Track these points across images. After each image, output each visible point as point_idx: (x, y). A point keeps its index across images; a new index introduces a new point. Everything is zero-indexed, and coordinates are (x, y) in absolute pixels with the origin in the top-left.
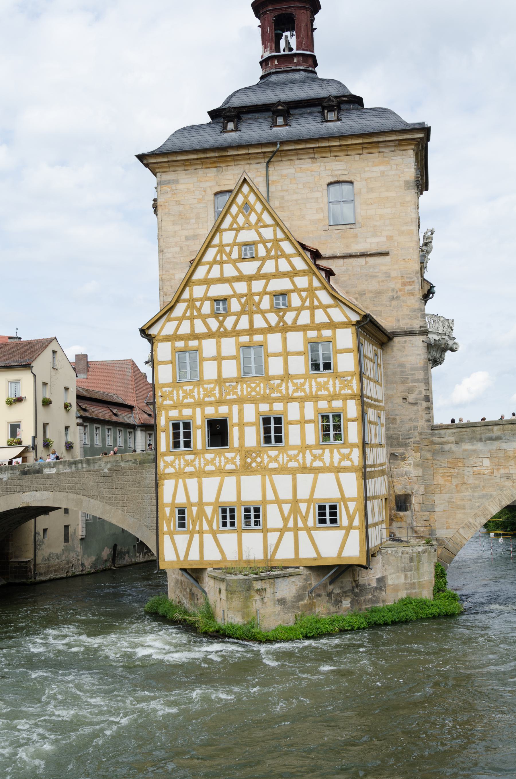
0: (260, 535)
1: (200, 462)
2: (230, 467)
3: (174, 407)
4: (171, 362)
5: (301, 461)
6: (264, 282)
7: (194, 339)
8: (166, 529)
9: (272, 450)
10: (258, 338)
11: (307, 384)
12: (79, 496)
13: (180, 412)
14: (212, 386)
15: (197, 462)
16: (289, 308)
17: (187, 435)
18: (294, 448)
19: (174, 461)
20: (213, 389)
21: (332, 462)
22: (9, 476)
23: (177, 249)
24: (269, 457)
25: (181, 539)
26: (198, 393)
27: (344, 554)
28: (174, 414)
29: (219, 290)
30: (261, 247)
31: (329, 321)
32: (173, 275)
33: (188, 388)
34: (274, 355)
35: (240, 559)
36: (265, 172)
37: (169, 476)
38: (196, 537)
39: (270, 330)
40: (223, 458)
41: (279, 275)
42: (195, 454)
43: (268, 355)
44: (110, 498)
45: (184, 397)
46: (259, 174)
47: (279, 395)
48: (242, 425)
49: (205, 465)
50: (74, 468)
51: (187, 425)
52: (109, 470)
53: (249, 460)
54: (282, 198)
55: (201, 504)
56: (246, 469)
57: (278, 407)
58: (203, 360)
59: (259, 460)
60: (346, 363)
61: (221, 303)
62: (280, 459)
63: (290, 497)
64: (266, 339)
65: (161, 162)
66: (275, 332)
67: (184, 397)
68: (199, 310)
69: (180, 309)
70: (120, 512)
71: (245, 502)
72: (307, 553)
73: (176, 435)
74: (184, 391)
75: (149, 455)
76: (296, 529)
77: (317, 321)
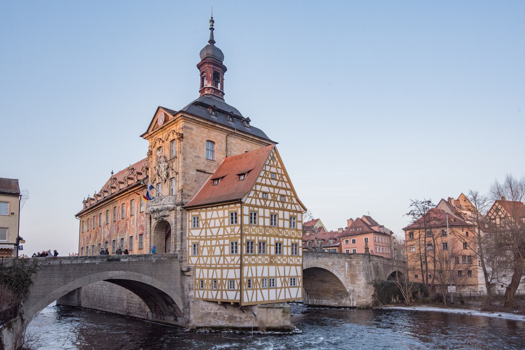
0: (275, 290)
2: (266, 262)
3: (249, 235)
4: (248, 215)
10: (276, 211)
18: (285, 256)
25: (250, 292)
26: (257, 230)
28: (248, 238)
33: (254, 228)
34: (281, 219)
37: (246, 265)
38: (255, 291)
39: (279, 209)
41: (282, 188)
43: (279, 219)
45: (252, 231)
48: (270, 245)
51: (252, 243)
54: (231, 152)
55: (257, 277)
56: (271, 263)
57: (281, 239)
58: (259, 217)
60: (299, 226)
63: (283, 275)
67: (252, 231)
72: (288, 297)
73: (248, 247)
74: (253, 229)
76: (285, 288)
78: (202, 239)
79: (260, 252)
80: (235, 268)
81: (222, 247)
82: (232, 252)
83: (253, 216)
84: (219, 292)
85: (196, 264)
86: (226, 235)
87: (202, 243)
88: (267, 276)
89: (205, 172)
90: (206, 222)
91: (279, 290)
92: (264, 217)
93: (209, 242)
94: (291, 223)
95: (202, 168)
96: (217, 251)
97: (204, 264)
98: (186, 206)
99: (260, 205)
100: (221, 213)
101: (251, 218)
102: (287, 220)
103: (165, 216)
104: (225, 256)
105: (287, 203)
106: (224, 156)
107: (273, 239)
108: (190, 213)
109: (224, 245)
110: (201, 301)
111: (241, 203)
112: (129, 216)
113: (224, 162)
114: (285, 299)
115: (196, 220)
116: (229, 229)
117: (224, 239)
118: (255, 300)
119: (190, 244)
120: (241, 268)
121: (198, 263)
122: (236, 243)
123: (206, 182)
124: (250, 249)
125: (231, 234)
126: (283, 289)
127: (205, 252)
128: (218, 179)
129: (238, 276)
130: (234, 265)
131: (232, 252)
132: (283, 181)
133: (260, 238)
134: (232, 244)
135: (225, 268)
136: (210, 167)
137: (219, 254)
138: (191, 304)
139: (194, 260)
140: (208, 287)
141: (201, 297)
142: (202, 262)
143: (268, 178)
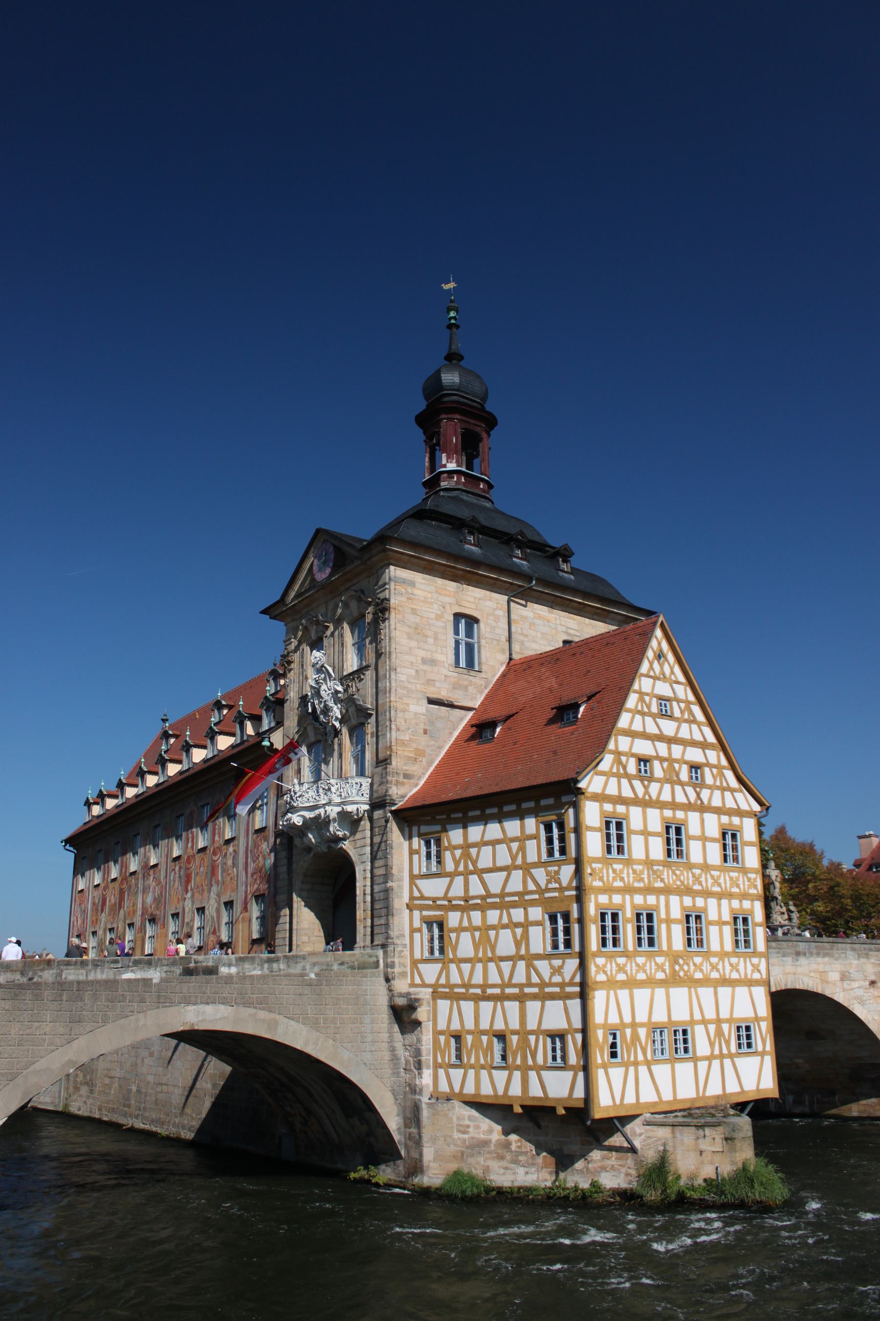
0: (691, 1065)
1: (631, 967)
2: (660, 976)
5: (721, 971)
6: (681, 747)
7: (622, 804)
8: (599, 1061)
9: (697, 956)
10: (680, 814)
11: (722, 877)
12: (272, 1015)
13: (610, 898)
14: (641, 867)
15: (628, 968)
16: (703, 785)
17: (615, 930)
18: (715, 954)
19: (605, 966)
20: (642, 872)
21: (746, 974)
22: (164, 975)
23: (413, 672)
24: (695, 964)
25: (616, 1073)
26: (629, 876)
27: (762, 1086)
28: (603, 899)
29: (644, 747)
30: (675, 704)
31: (736, 807)
32: (408, 704)
34: (695, 838)
35: (675, 1099)
36: (506, 607)
39: (688, 807)
40: (653, 964)
41: (693, 743)
42: (627, 956)
43: (690, 838)
44: (317, 1019)
45: (614, 879)
46: (500, 606)
47: (700, 888)
49: (637, 972)
50: (266, 971)
51: (615, 917)
52: (316, 975)
53: (677, 968)
54: (522, 643)
55: (634, 1025)
56: (673, 980)
57: (700, 902)
58: (631, 832)
59: (686, 968)
60: (751, 857)
61: (642, 763)
62: (704, 968)
63: (714, 1016)
64: (686, 816)
65: (402, 553)
66: (695, 810)
67: (614, 879)
68: (625, 767)
69: (607, 762)
70: (331, 1042)
71: (676, 1022)
72: (732, 1087)
73: (603, 930)
74: (614, 871)
75: (371, 956)
76: (722, 1056)
77: (727, 806)
78: (455, 908)
79: (640, 945)
80: (565, 997)
81: (519, 931)
82: (555, 946)
83: (615, 832)
84: (517, 1075)
85: (435, 987)
86: (532, 892)
87: (453, 919)
88: (665, 1019)
89: (451, 706)
90: (466, 855)
91: (703, 1066)
92: (646, 833)
93: (476, 917)
94: (725, 849)
95: (444, 694)
96: (506, 943)
97: (463, 985)
98: (400, 804)
99: (632, 795)
100: (513, 827)
101: (608, 836)
102: (713, 840)
103: (339, 840)
104: (530, 959)
105: (709, 787)
106: (505, 658)
107: (674, 900)
108: (415, 829)
109: (526, 925)
110: (456, 1104)
111: (580, 792)
112: (222, 842)
113: (503, 675)
114: (725, 1095)
115: (434, 849)
116: (540, 874)
117: (525, 905)
118: (634, 1101)
119: (417, 924)
120: (583, 996)
121: (443, 981)
122: (566, 917)
123: (456, 734)
124: (609, 935)
125: (548, 890)
126: (716, 1063)
127: (465, 946)
128: (493, 725)
129: (577, 1024)
130: (562, 985)
131: (555, 946)
132: (693, 721)
133: (639, 899)
134: (553, 919)
135: (534, 997)
136: (466, 688)
137: (512, 951)
138: (425, 1113)
139: (431, 972)
140: (477, 1058)
141: (457, 1089)
142: (455, 979)
143: (650, 714)
